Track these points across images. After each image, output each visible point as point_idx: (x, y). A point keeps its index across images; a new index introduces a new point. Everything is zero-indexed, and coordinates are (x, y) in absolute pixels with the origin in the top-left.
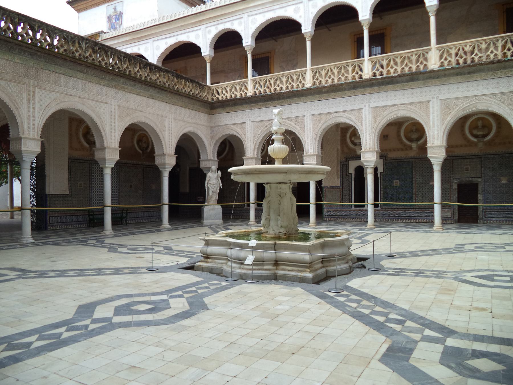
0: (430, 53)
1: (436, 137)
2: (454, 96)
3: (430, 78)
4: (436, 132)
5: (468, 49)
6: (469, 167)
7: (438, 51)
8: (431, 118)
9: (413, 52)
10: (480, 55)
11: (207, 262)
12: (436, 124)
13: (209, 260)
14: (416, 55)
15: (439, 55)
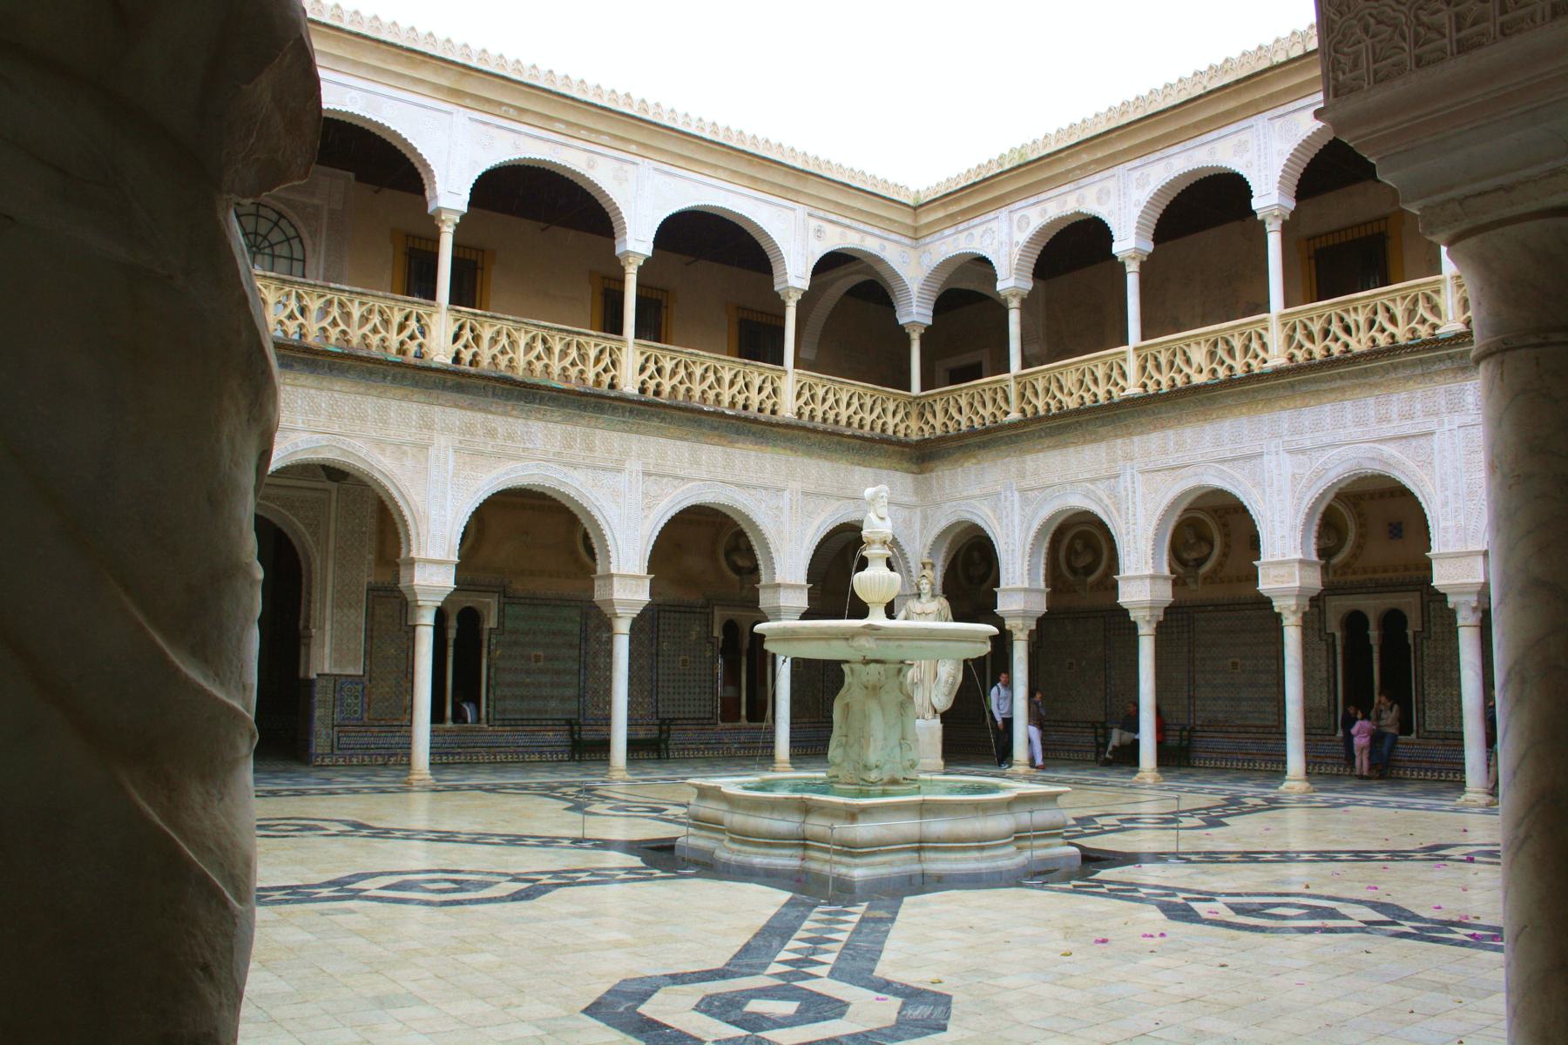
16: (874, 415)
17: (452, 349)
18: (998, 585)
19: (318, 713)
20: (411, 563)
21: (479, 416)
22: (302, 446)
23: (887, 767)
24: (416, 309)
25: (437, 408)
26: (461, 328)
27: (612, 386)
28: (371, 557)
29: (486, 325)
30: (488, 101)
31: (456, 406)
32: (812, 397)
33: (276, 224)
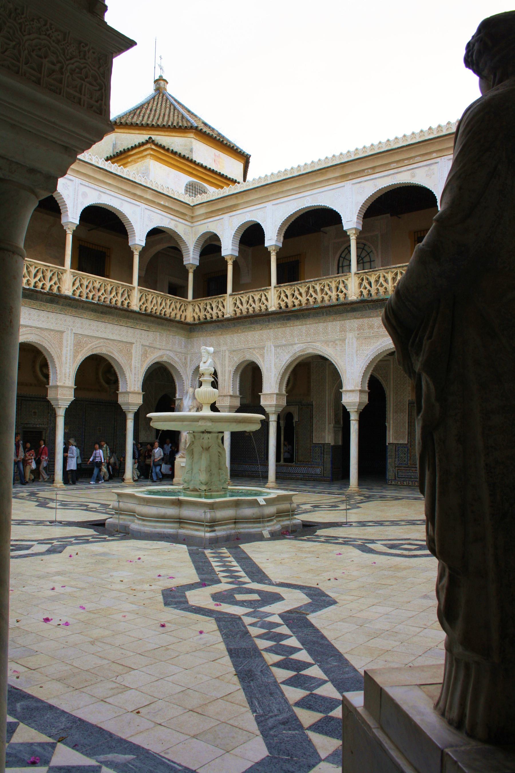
0: (65, 275)
1: (67, 375)
2: (86, 333)
3: (69, 305)
4: (68, 371)
5: (97, 285)
6: (37, 411)
7: (72, 277)
8: (64, 352)
9: (49, 266)
10: (106, 296)
11: (214, 531)
12: (68, 361)
13: (216, 528)
14: (51, 271)
15: (73, 281)
19: (389, 461)
20: (361, 391)
21: (366, 320)
22: (297, 350)
23: (192, 482)
24: (341, 279)
25: (348, 321)
28: (410, 388)
30: (358, 172)
31: (355, 318)
33: (363, 249)
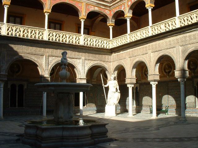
16: (102, 44)
17: (7, 33)
18: (126, 77)
26: (9, 28)
27: (42, 38)
29: (14, 27)
32: (87, 40)
